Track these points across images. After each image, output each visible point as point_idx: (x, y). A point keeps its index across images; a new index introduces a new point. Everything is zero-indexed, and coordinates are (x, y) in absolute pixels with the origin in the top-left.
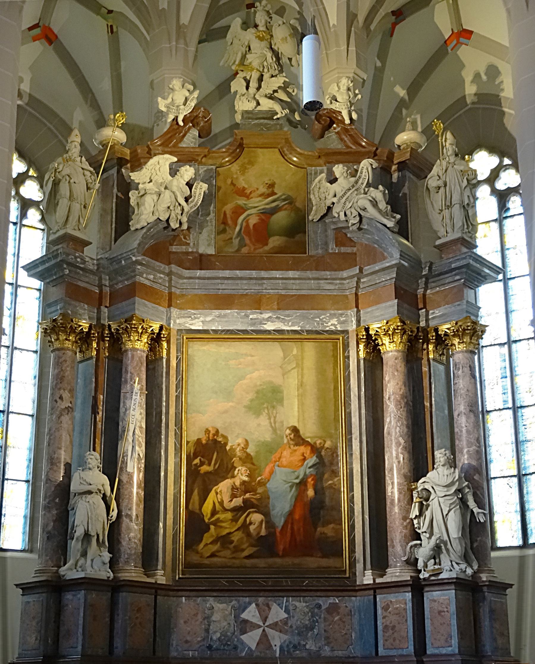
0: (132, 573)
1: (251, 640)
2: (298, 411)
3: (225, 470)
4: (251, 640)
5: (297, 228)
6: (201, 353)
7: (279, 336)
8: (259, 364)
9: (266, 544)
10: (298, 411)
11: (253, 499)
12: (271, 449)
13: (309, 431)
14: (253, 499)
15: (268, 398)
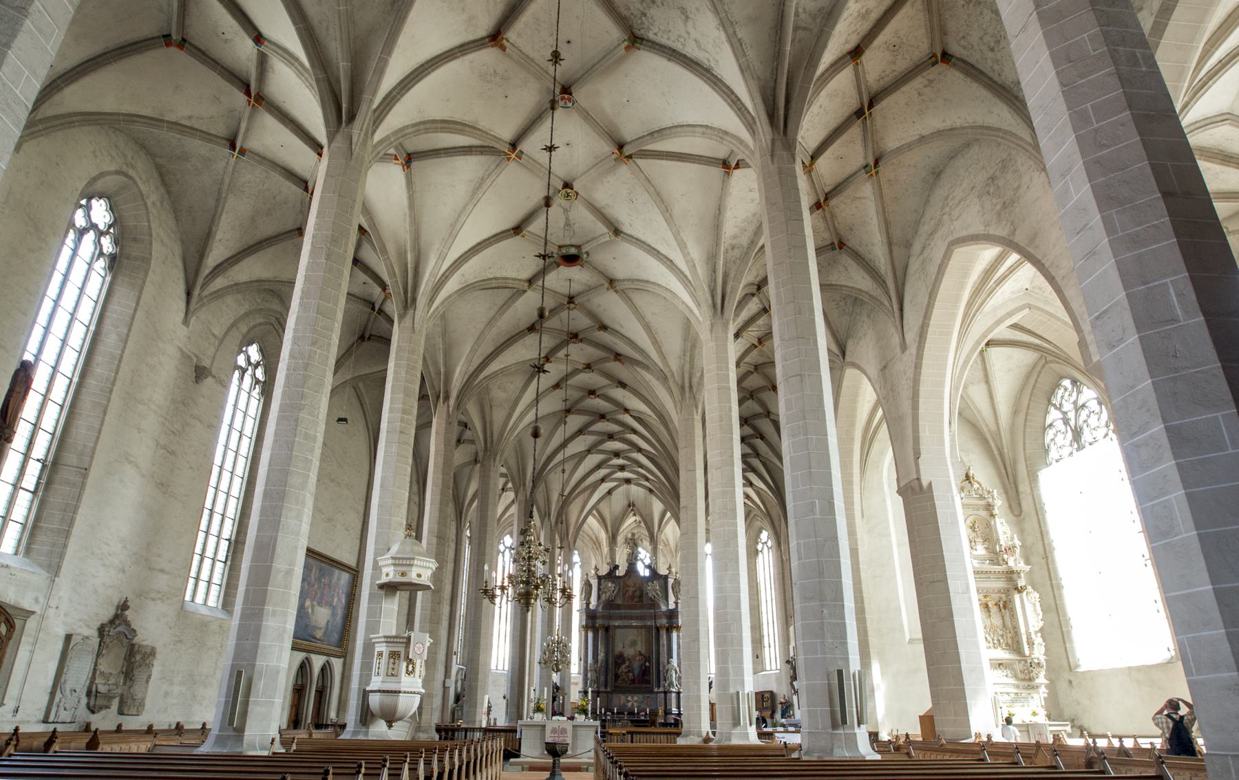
0: (602, 689)
1: (630, 704)
2: (641, 647)
3: (624, 662)
4: (630, 704)
5: (641, 596)
6: (618, 631)
7: (636, 627)
8: (631, 635)
9: (633, 681)
10: (641, 647)
11: (630, 670)
12: (634, 657)
13: (643, 652)
14: (630, 670)
15: (634, 643)
